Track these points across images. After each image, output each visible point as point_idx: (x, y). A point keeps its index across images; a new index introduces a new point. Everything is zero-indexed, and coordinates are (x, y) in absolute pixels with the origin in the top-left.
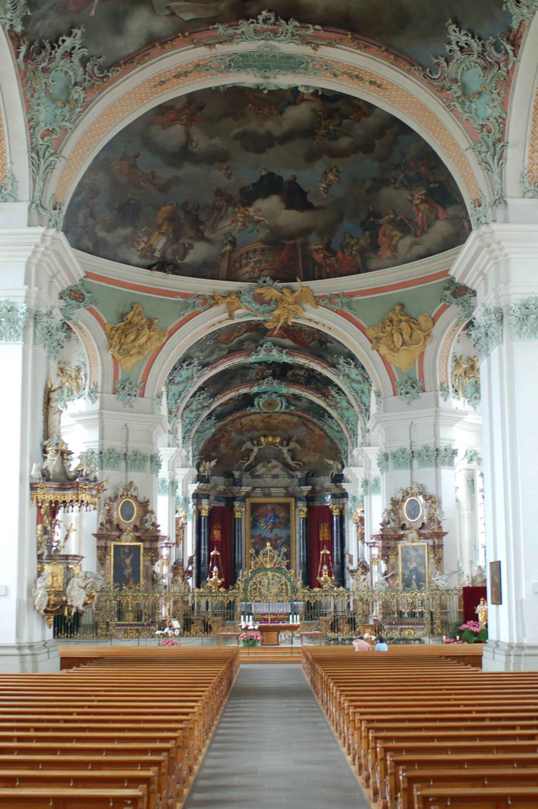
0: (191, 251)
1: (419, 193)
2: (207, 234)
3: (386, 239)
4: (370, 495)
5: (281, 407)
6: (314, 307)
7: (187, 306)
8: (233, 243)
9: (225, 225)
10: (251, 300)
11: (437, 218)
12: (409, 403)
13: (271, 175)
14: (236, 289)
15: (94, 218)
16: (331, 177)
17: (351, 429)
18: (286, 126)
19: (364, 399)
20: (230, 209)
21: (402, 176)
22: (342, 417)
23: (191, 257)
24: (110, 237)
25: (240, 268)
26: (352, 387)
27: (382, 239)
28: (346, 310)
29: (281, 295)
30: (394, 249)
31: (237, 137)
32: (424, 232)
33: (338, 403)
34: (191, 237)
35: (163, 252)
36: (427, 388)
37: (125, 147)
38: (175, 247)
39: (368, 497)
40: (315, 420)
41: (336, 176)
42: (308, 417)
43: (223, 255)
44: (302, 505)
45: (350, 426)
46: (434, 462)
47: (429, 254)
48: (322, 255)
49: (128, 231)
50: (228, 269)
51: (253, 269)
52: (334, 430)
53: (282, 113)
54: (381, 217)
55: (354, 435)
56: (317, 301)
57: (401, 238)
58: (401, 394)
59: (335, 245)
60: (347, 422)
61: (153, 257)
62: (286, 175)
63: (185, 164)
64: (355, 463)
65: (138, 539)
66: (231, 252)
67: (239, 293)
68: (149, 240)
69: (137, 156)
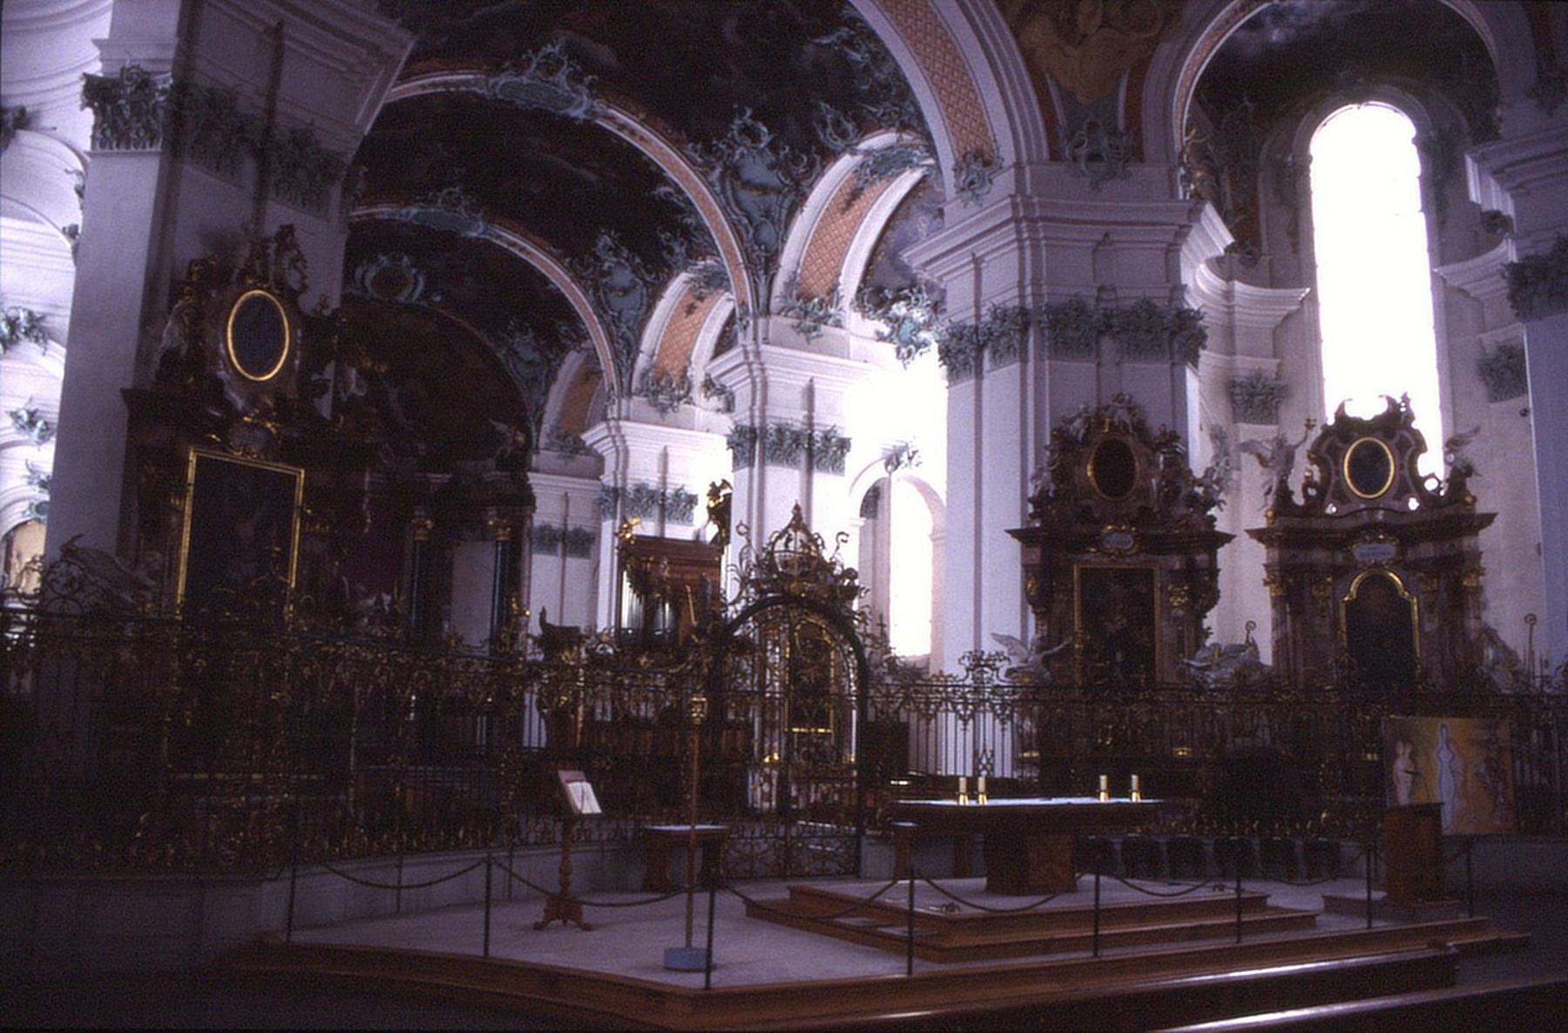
4: (763, 464)
5: (411, 295)
12: (1095, 186)
17: (622, 337)
19: (767, 233)
22: (601, 307)
26: (738, 204)
33: (604, 274)
36: (1150, 149)
39: (756, 470)
40: (482, 336)
42: (466, 324)
44: (423, 513)
45: (624, 329)
46: (1167, 348)
52: (521, 360)
55: (629, 353)
58: (1075, 159)
60: (616, 321)
64: (623, 414)
65: (288, 451)
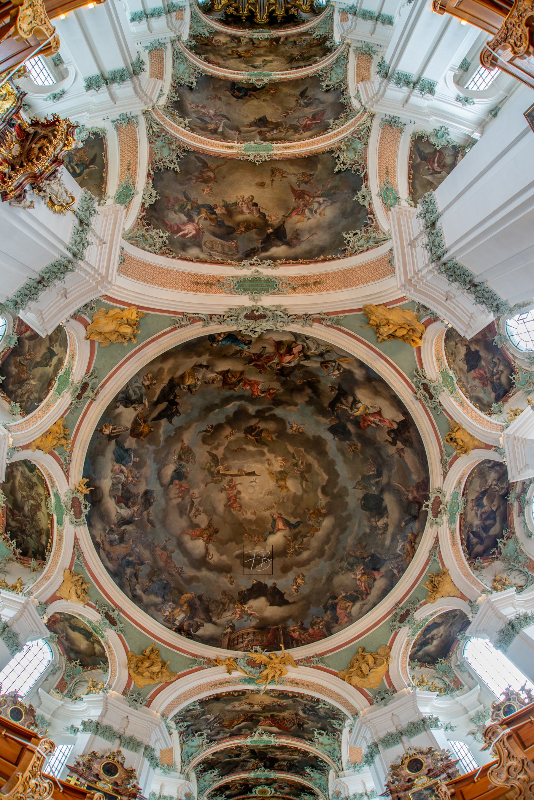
0: (202, 628)
1: (359, 571)
2: (214, 619)
3: (342, 611)
6: (295, 667)
7: (194, 662)
8: (233, 627)
9: (228, 616)
10: (246, 665)
11: (375, 580)
13: (260, 583)
14: (234, 656)
15: (137, 579)
16: (299, 581)
18: (268, 550)
20: (231, 605)
21: (346, 564)
23: (201, 632)
24: (145, 598)
25: (237, 644)
27: (339, 611)
28: (320, 665)
29: (269, 660)
30: (349, 616)
31: (238, 557)
32: (368, 594)
34: (203, 619)
35: (182, 623)
37: (166, 541)
38: (191, 622)
41: (303, 580)
43: (225, 634)
47: (374, 605)
48: (297, 633)
49: (159, 600)
50: (228, 645)
51: (247, 645)
53: (266, 540)
54: (337, 598)
56: (297, 663)
57: (353, 606)
59: (307, 624)
61: (174, 624)
62: (269, 583)
63: (203, 569)
66: (231, 633)
67: (236, 660)
68: (172, 611)
69: (173, 552)
